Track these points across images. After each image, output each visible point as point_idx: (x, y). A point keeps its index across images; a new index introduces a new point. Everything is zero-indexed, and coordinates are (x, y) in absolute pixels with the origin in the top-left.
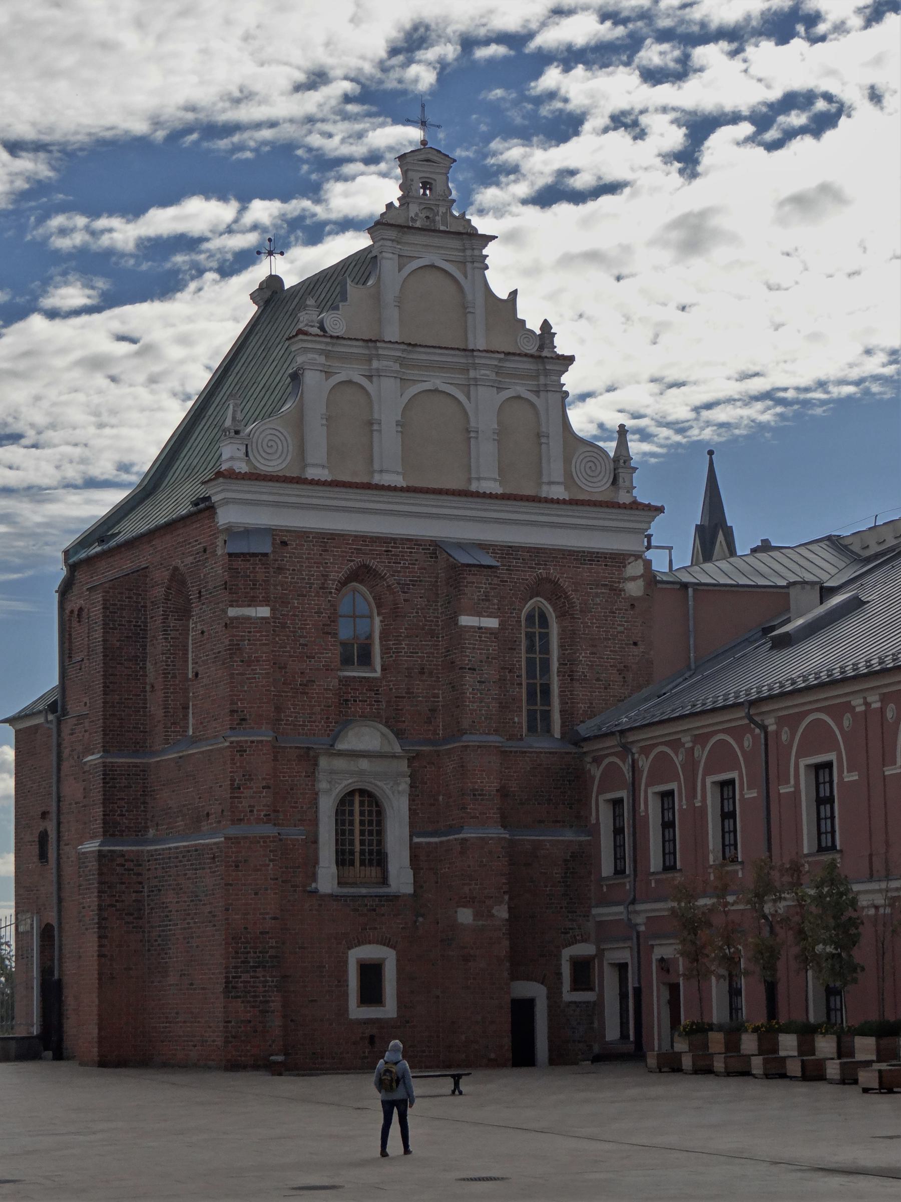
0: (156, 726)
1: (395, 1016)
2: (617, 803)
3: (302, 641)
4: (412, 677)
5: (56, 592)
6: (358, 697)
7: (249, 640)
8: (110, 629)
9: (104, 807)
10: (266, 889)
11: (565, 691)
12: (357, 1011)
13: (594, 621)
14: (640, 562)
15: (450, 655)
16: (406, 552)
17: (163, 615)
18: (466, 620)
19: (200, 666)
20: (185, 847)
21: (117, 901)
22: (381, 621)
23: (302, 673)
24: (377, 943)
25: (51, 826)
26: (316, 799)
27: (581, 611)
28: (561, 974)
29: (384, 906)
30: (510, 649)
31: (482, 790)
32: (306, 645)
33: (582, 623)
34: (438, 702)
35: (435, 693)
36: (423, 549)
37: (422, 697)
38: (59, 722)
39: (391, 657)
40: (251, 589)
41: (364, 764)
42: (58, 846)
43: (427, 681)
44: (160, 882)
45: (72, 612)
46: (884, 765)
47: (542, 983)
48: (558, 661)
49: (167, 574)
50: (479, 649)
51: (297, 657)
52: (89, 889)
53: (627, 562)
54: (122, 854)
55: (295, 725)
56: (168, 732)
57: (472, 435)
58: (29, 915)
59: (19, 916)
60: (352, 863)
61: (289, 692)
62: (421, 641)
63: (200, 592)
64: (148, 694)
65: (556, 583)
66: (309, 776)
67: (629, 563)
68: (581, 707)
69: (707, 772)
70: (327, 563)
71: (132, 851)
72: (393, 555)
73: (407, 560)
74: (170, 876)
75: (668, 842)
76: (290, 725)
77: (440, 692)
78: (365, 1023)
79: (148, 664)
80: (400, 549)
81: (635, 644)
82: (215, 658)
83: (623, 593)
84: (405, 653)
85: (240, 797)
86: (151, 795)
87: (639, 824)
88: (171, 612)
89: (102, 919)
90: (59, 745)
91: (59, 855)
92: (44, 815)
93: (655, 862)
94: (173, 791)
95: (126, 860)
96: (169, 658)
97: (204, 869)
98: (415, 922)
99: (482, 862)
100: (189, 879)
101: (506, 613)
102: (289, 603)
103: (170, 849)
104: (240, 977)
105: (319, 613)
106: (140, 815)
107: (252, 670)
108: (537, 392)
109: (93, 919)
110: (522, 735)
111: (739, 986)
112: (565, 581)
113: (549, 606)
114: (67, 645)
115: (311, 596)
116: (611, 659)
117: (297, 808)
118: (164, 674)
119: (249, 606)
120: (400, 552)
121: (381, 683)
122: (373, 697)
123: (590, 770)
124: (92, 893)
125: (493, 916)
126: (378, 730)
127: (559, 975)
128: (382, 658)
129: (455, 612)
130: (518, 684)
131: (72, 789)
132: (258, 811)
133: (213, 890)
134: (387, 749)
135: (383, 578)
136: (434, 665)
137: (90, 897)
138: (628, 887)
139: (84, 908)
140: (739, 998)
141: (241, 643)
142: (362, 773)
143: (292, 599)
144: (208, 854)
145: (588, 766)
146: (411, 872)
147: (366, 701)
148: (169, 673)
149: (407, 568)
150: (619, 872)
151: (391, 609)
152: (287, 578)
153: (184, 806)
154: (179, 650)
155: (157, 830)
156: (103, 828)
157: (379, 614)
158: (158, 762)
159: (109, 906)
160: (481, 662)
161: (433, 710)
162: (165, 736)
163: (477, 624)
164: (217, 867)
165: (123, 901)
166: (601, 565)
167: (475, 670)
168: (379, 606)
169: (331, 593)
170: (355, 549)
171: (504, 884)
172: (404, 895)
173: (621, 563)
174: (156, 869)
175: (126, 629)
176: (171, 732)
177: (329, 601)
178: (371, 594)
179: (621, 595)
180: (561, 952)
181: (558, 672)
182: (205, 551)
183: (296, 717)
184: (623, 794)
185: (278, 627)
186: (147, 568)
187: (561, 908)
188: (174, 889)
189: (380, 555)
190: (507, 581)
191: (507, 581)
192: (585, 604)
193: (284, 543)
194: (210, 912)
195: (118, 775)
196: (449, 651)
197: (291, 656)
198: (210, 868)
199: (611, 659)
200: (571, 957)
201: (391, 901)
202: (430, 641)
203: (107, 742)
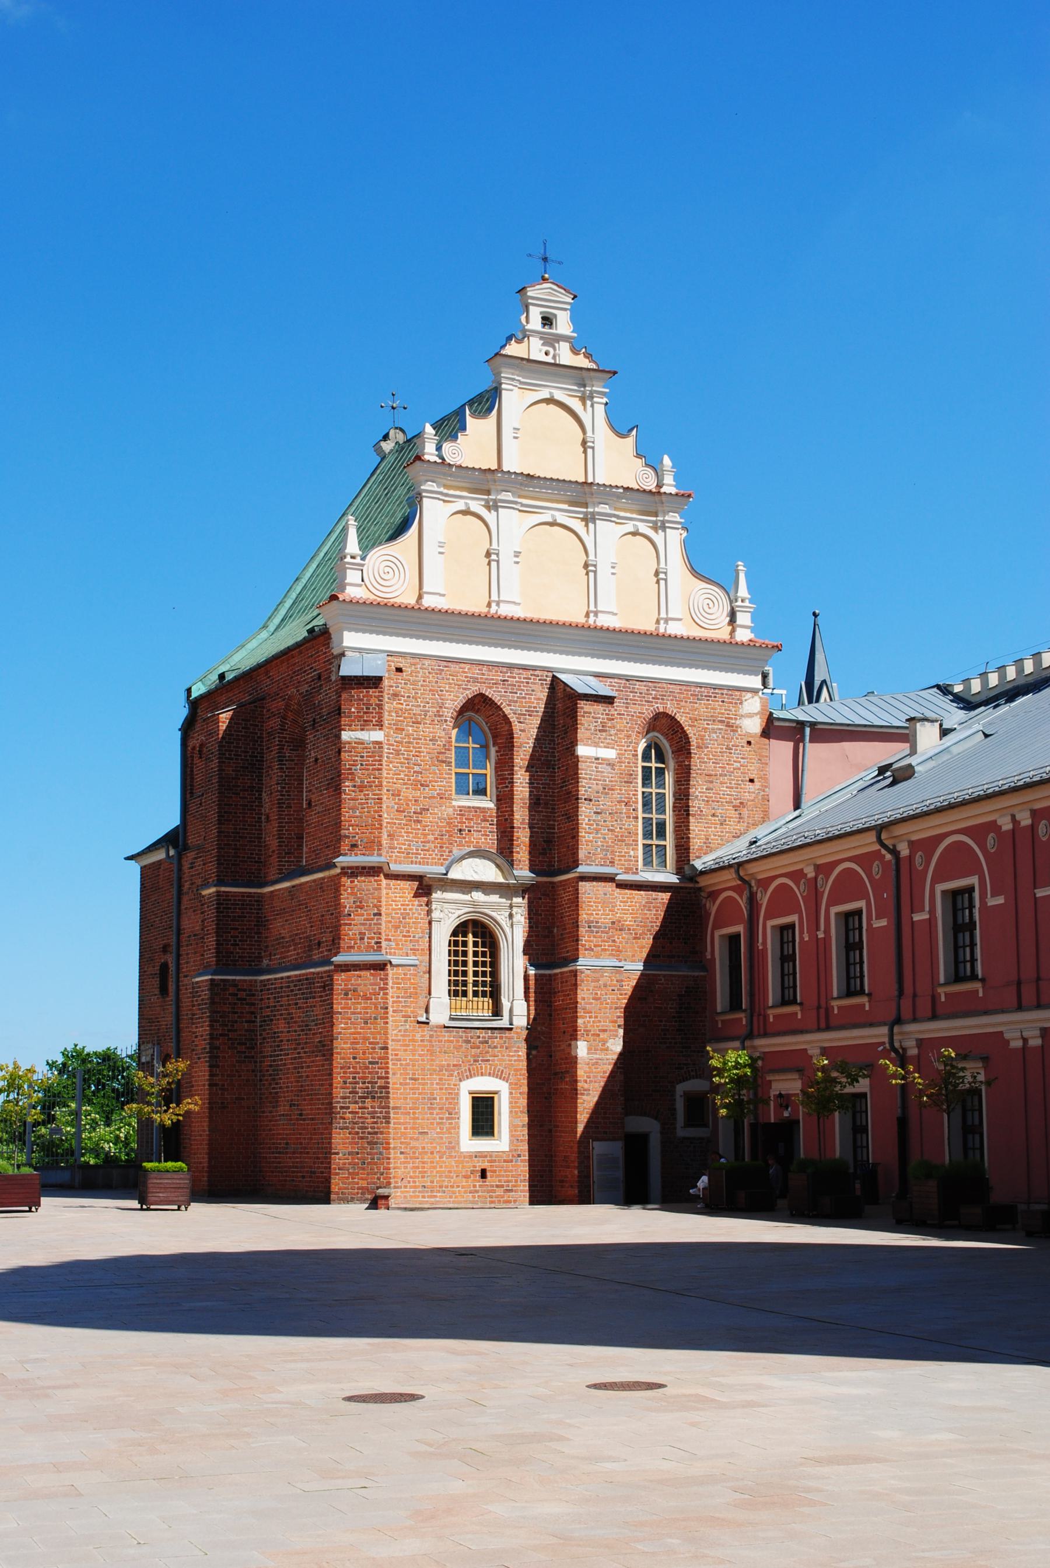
0: (271, 856)
1: (507, 1150)
2: (734, 939)
3: (417, 768)
5: (180, 730)
7: (362, 765)
8: (226, 758)
9: (217, 936)
10: (375, 1018)
11: (681, 826)
12: (469, 1143)
13: (711, 757)
14: (756, 698)
15: (566, 786)
16: (523, 682)
17: (278, 745)
19: (314, 794)
20: (296, 976)
21: (229, 1031)
22: (497, 752)
23: (416, 801)
24: (490, 1075)
25: (171, 959)
27: (698, 747)
28: (675, 1109)
30: (625, 782)
31: (597, 922)
32: (421, 773)
33: (698, 758)
34: (554, 833)
36: (540, 680)
37: (538, 828)
38: (180, 856)
39: (507, 787)
40: (366, 713)
41: (478, 896)
42: (178, 978)
43: (542, 812)
44: (272, 1011)
45: (194, 748)
46: (1035, 888)
47: (656, 1119)
48: (674, 796)
49: (282, 704)
50: (595, 780)
51: (412, 784)
52: (202, 1018)
53: (744, 699)
55: (408, 853)
56: (282, 861)
57: (591, 568)
58: (150, 1045)
59: (142, 1047)
60: (465, 994)
61: (402, 820)
62: (537, 772)
63: (314, 720)
64: (263, 824)
65: (672, 719)
69: (832, 902)
70: (441, 691)
71: (245, 981)
72: (508, 685)
73: (523, 690)
74: (281, 1006)
75: (786, 976)
76: (403, 853)
77: (556, 823)
78: (476, 1157)
79: (264, 794)
80: (517, 679)
81: (752, 781)
82: (328, 784)
83: (739, 730)
85: (350, 924)
86: (265, 926)
87: (756, 956)
88: (286, 742)
89: (213, 1047)
90: (180, 879)
91: (178, 986)
92: (165, 949)
93: (772, 995)
94: (286, 921)
95: (239, 990)
96: (284, 788)
97: (314, 997)
99: (597, 994)
100: (300, 1008)
101: (624, 746)
102: (403, 730)
103: (282, 978)
104: (348, 1108)
106: (254, 945)
107: (365, 795)
108: (655, 529)
109: (205, 1048)
110: (637, 869)
111: (864, 1123)
112: (682, 716)
113: (665, 742)
114: (188, 781)
116: (727, 795)
117: (410, 936)
118: (279, 803)
119: (362, 730)
120: (516, 682)
122: (488, 828)
123: (705, 905)
124: (205, 1022)
125: (607, 1049)
127: (673, 1111)
128: (497, 788)
129: (572, 742)
130: (634, 818)
131: (191, 923)
132: (368, 938)
133: (323, 1019)
135: (499, 708)
136: (550, 796)
137: (202, 1027)
138: (744, 1023)
139: (196, 1037)
140: (864, 1136)
141: (354, 767)
142: (474, 904)
143: (407, 725)
144: (318, 982)
145: (704, 900)
147: (480, 831)
148: (284, 803)
149: (525, 698)
150: (735, 1004)
151: (507, 739)
152: (402, 704)
153: (296, 935)
154: (294, 780)
155: (270, 960)
156: (216, 957)
157: (494, 745)
158: (272, 892)
159: (221, 1035)
160: (598, 792)
162: (279, 865)
163: (594, 755)
164: (327, 995)
165: (236, 1030)
166: (718, 701)
167: (590, 800)
168: (495, 737)
169: (446, 721)
170: (471, 677)
171: (619, 1017)
173: (738, 699)
174: (269, 999)
175: (242, 760)
176: (285, 861)
179: (737, 731)
180: (675, 1087)
182: (319, 677)
183: (409, 845)
184: (740, 928)
185: (392, 753)
186: (264, 699)
187: (676, 1043)
188: (285, 1019)
189: (496, 684)
190: (623, 715)
191: (623, 715)
192: (702, 739)
193: (399, 670)
194: (320, 1042)
195: (232, 904)
196: (565, 782)
197: (405, 784)
198: (321, 996)
199: (727, 795)
200: (685, 1093)
203: (222, 872)
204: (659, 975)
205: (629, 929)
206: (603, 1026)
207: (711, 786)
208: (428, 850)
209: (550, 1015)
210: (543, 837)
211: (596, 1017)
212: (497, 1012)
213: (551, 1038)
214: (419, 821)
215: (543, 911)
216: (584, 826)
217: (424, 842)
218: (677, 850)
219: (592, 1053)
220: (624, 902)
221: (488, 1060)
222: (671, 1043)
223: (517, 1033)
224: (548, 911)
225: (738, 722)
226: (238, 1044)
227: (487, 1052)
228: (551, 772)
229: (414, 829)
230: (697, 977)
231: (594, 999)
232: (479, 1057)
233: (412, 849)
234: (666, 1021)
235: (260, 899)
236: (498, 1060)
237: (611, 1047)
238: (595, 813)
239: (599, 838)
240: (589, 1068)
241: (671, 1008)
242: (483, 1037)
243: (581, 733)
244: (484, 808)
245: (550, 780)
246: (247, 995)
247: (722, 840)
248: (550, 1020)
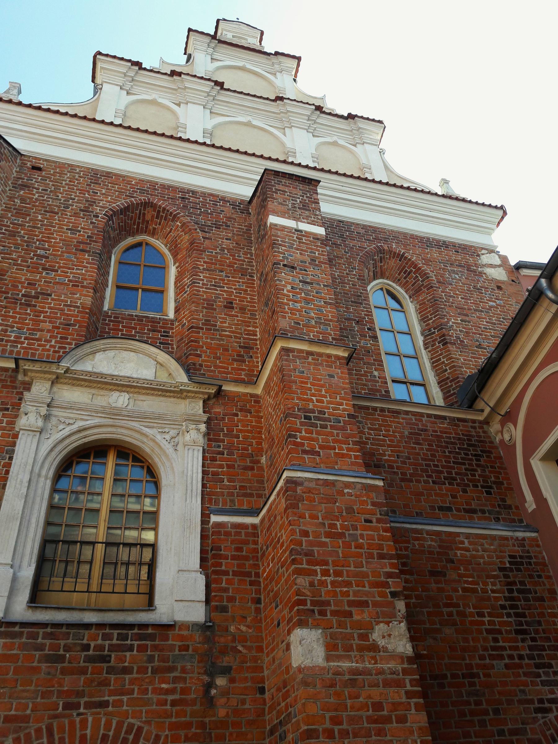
4: (215, 309)
18: (273, 219)
23: (29, 284)
26: (14, 444)
29: (130, 648)
34: (256, 340)
35: (251, 331)
37: (229, 331)
43: (237, 316)
48: (422, 334)
66: (7, 409)
77: (258, 330)
84: (203, 284)
98: (210, 685)
105: (74, 230)
115: (66, 215)
121: (173, 324)
122: (159, 339)
125: (374, 648)
126: (150, 356)
134: (163, 377)
135: (175, 218)
136: (247, 302)
146: (201, 580)
161: (247, 348)
168: (175, 256)
171: (389, 575)
172: (184, 626)
177: (92, 223)
178: (166, 246)
181: (425, 344)
197: (14, 265)
201: (151, 637)
202: (240, 278)
204: (458, 534)
205: (391, 467)
206: (356, 593)
207: (467, 319)
208: (37, 340)
209: (258, 601)
210: (237, 342)
211: (338, 574)
212: (150, 604)
213: (260, 649)
214: (29, 305)
215: (241, 431)
216: (285, 292)
217: (33, 330)
218: (440, 387)
219: (339, 658)
220: (375, 429)
221: (105, 704)
222: (511, 657)
223: (182, 638)
224: (248, 431)
227: (105, 683)
228: (248, 279)
229: (19, 313)
230: (524, 539)
231: (328, 535)
232: (79, 694)
233: (10, 336)
234: (490, 615)
236: (132, 702)
237: (381, 643)
238: (300, 281)
240: (338, 695)
241: (493, 591)
242: (97, 648)
243: (271, 205)
244: (152, 318)
245: (246, 287)
248: (258, 610)
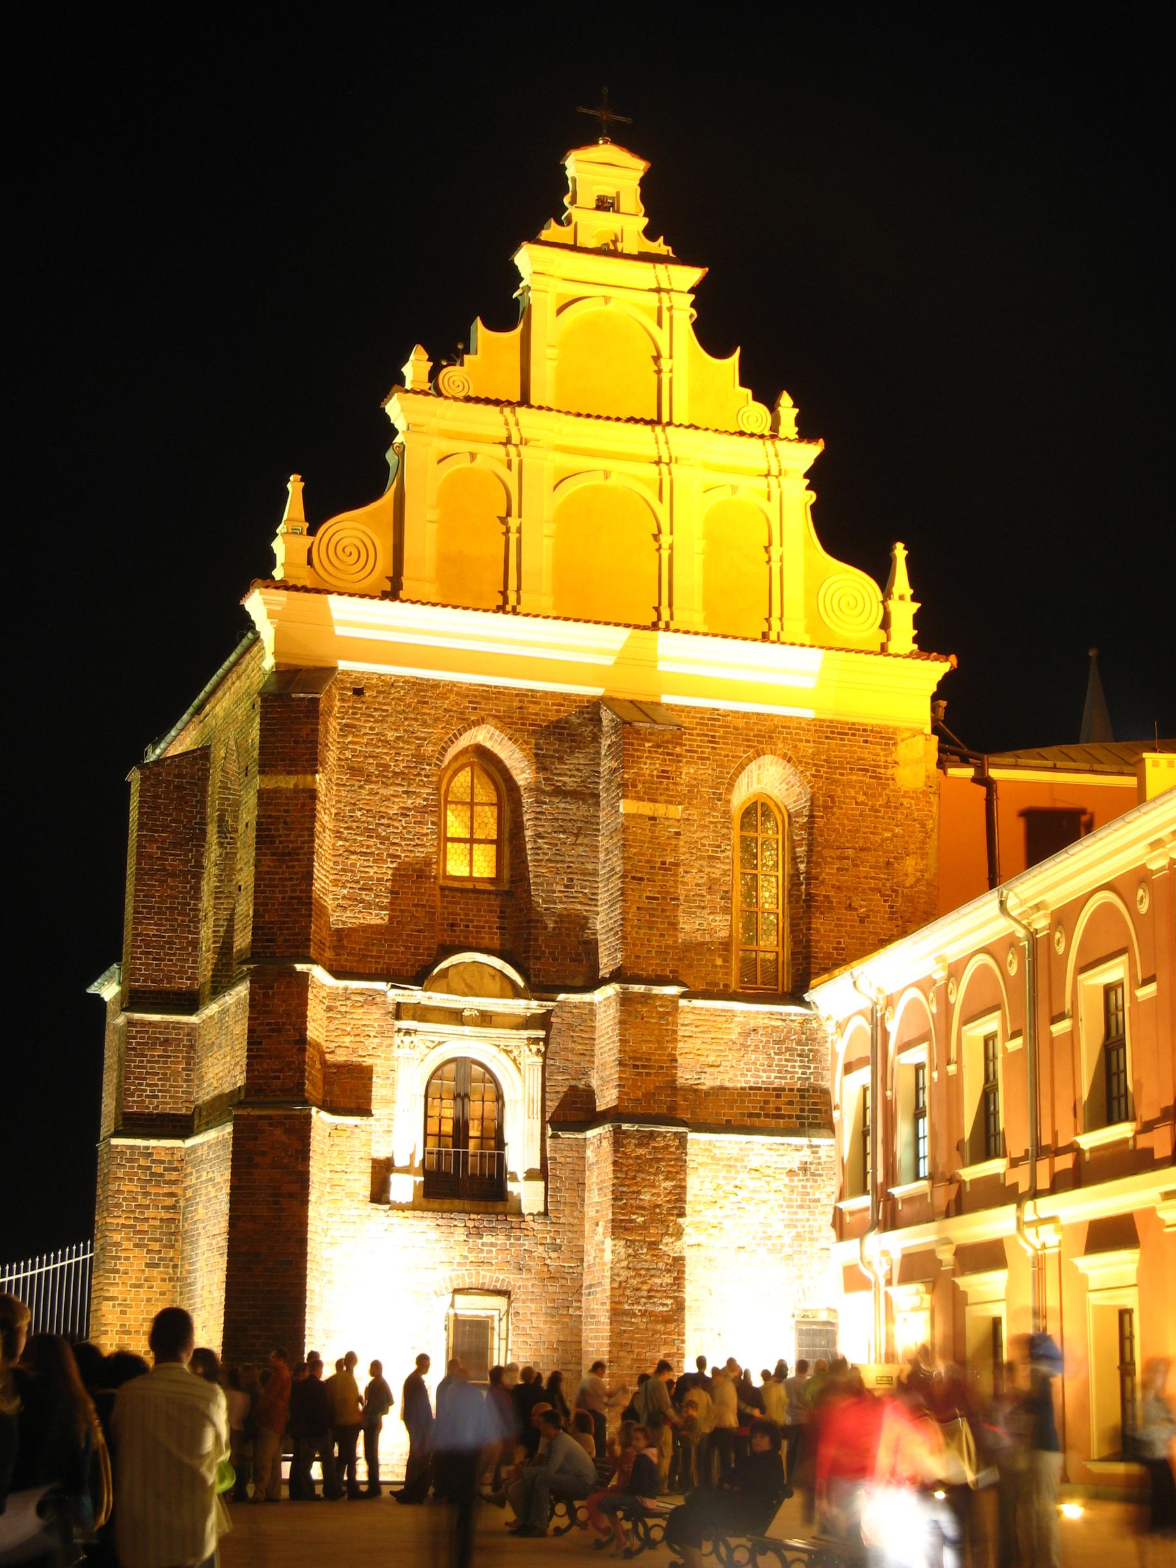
6: (472, 921)
13: (846, 822)
54: (147, 1153)
67: (903, 740)
68: (822, 948)
79: (204, 883)
95: (153, 1161)
163: (650, 814)
199: (872, 878)
225: (890, 772)
226: (150, 1240)
235: (192, 1030)
239: (654, 935)
246: (165, 1169)
247: (862, 944)
